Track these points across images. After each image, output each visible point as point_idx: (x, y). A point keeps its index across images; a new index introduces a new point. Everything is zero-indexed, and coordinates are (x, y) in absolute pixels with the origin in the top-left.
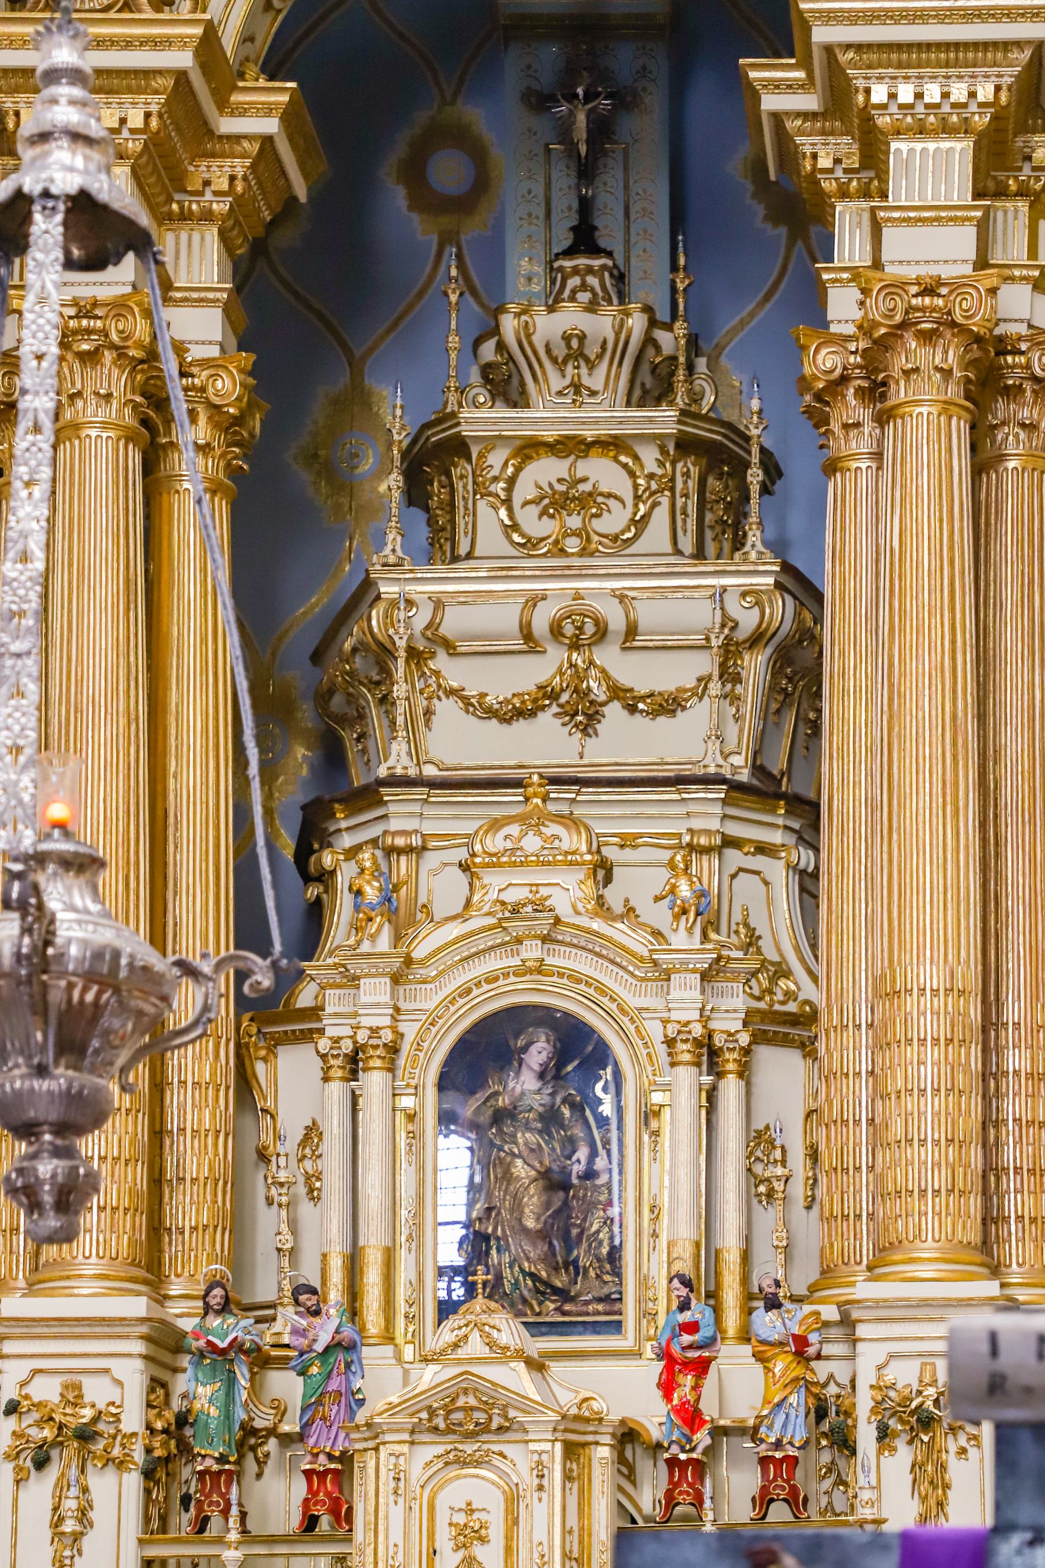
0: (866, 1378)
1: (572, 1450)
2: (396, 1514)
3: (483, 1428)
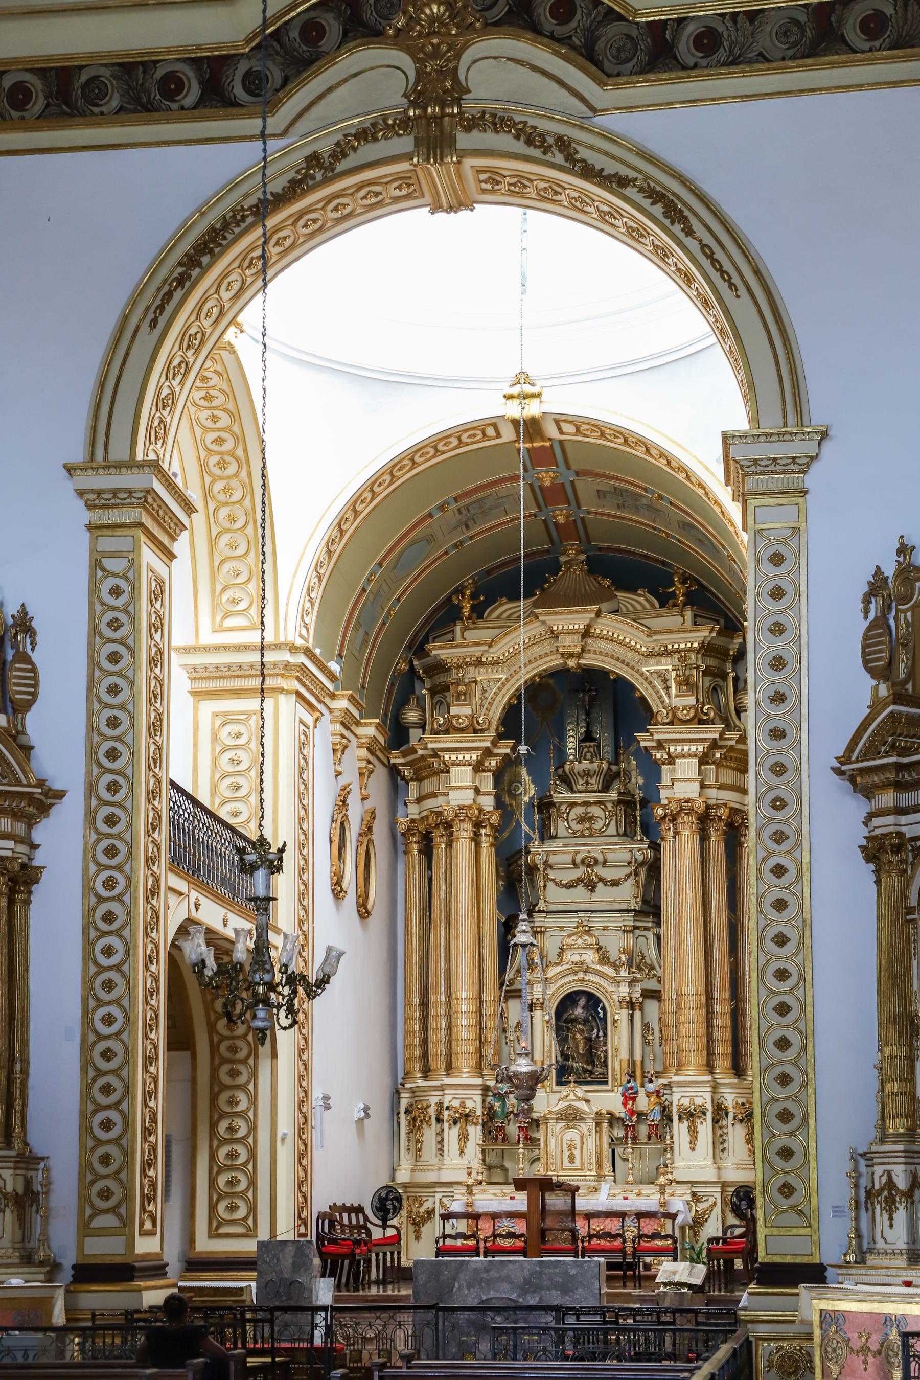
0: (675, 1103)
1: (598, 1125)
2: (553, 1141)
3: (574, 1120)
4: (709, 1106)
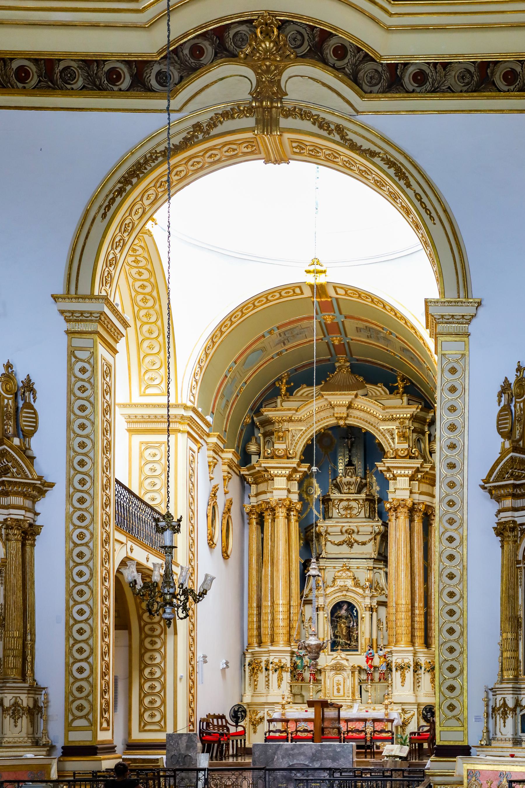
4: (412, 663)
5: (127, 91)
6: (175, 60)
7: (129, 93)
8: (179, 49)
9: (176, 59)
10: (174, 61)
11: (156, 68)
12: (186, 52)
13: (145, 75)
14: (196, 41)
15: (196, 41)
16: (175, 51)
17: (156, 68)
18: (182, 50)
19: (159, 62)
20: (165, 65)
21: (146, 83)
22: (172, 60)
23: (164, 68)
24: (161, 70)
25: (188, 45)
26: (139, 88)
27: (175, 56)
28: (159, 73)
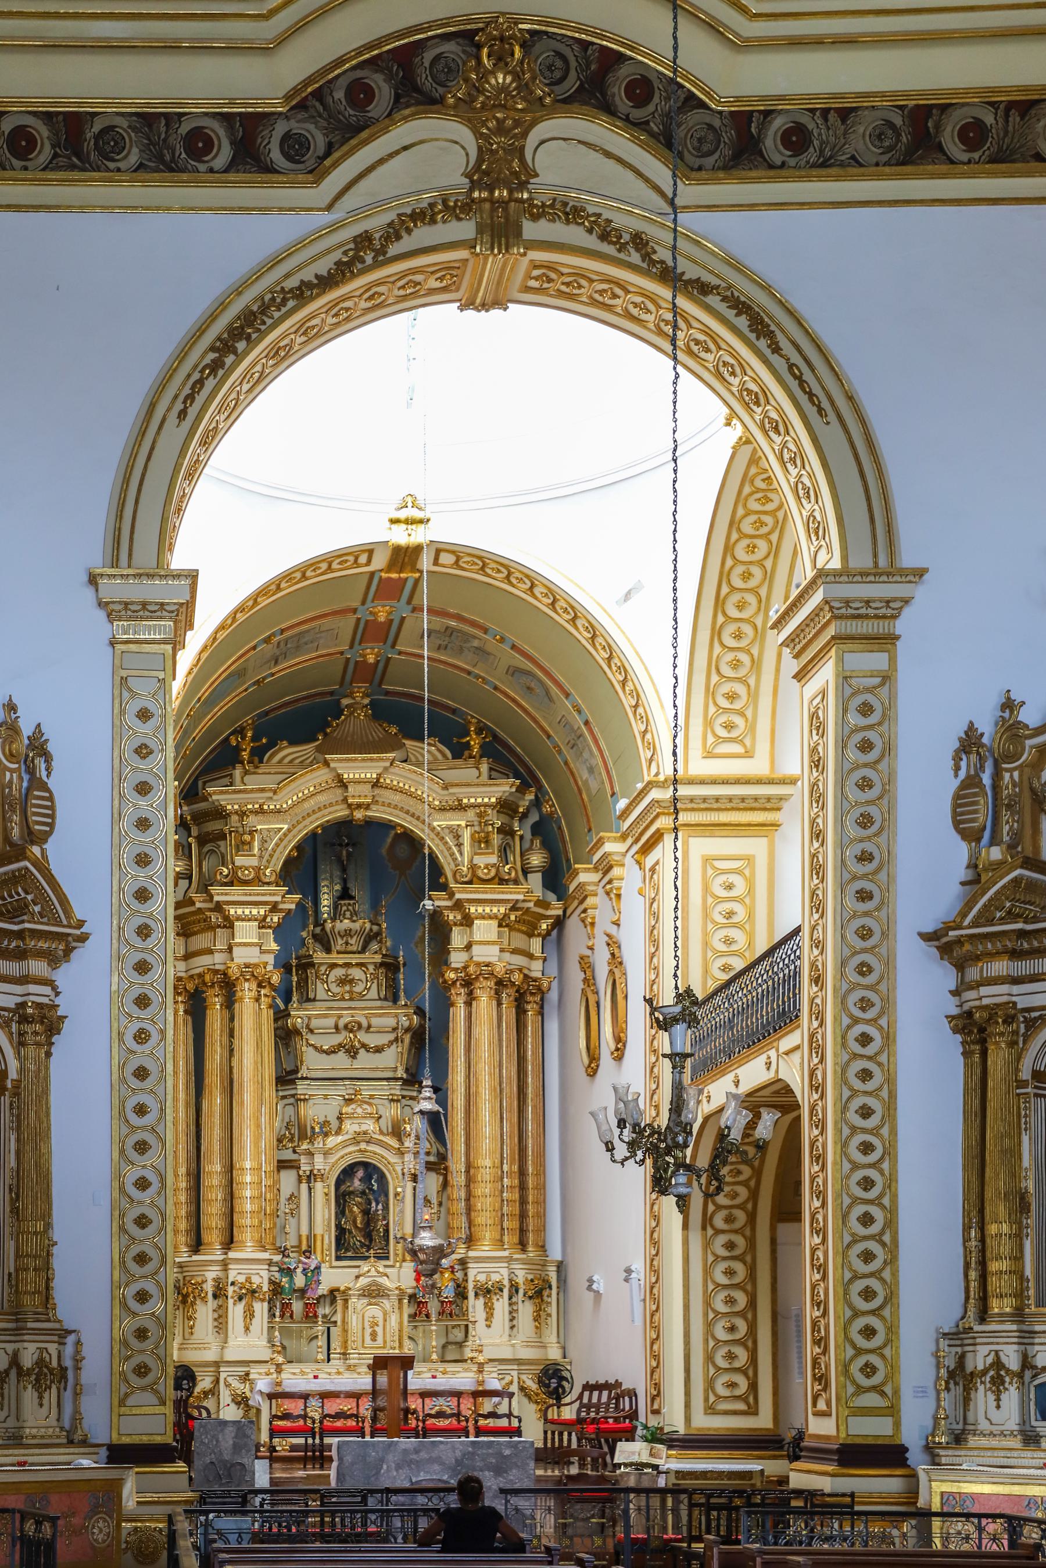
5: (225, 171)
6: (318, 112)
7: (231, 176)
8: (326, 90)
9: (321, 109)
10: (315, 114)
11: (281, 128)
12: (339, 94)
13: (259, 140)
14: (359, 74)
15: (359, 74)
16: (318, 94)
17: (281, 128)
18: (332, 92)
19: (286, 116)
20: (298, 122)
21: (262, 158)
22: (312, 111)
23: (295, 126)
24: (290, 130)
25: (343, 82)
26: (248, 167)
27: (317, 104)
28: (287, 137)
